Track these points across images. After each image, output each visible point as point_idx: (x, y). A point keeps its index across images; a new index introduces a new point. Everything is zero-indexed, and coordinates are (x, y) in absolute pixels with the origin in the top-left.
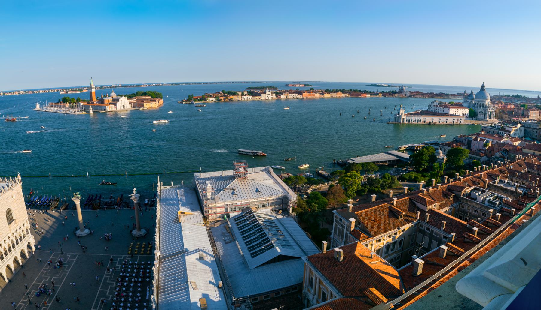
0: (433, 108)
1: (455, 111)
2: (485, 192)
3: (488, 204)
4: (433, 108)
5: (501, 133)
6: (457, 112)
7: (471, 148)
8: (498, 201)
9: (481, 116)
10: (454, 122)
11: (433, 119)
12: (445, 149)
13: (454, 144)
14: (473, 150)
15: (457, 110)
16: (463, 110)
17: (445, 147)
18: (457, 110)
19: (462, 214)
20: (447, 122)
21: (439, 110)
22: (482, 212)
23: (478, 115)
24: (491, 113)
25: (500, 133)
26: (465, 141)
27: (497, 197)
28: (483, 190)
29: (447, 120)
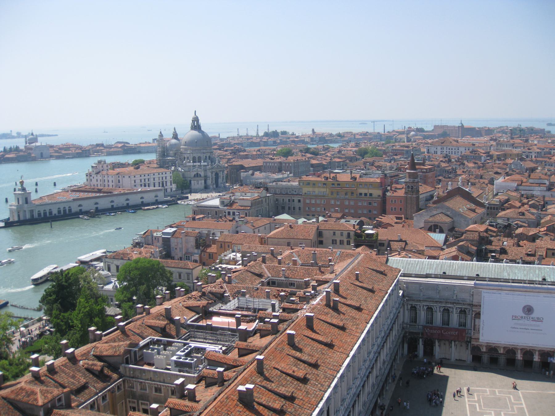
0: (95, 178)
1: (143, 181)
2: (170, 344)
3: (177, 369)
4: (95, 178)
5: (231, 213)
6: (147, 180)
7: (173, 254)
8: (196, 357)
9: (198, 183)
11: (97, 203)
12: (117, 267)
13: (133, 251)
14: (176, 257)
15: (149, 177)
16: (161, 176)
18: (149, 177)
19: (134, 402)
21: (110, 181)
22: (170, 389)
23: (192, 182)
24: (217, 174)
25: (229, 213)
26: (158, 241)
27: (198, 350)
28: (167, 341)
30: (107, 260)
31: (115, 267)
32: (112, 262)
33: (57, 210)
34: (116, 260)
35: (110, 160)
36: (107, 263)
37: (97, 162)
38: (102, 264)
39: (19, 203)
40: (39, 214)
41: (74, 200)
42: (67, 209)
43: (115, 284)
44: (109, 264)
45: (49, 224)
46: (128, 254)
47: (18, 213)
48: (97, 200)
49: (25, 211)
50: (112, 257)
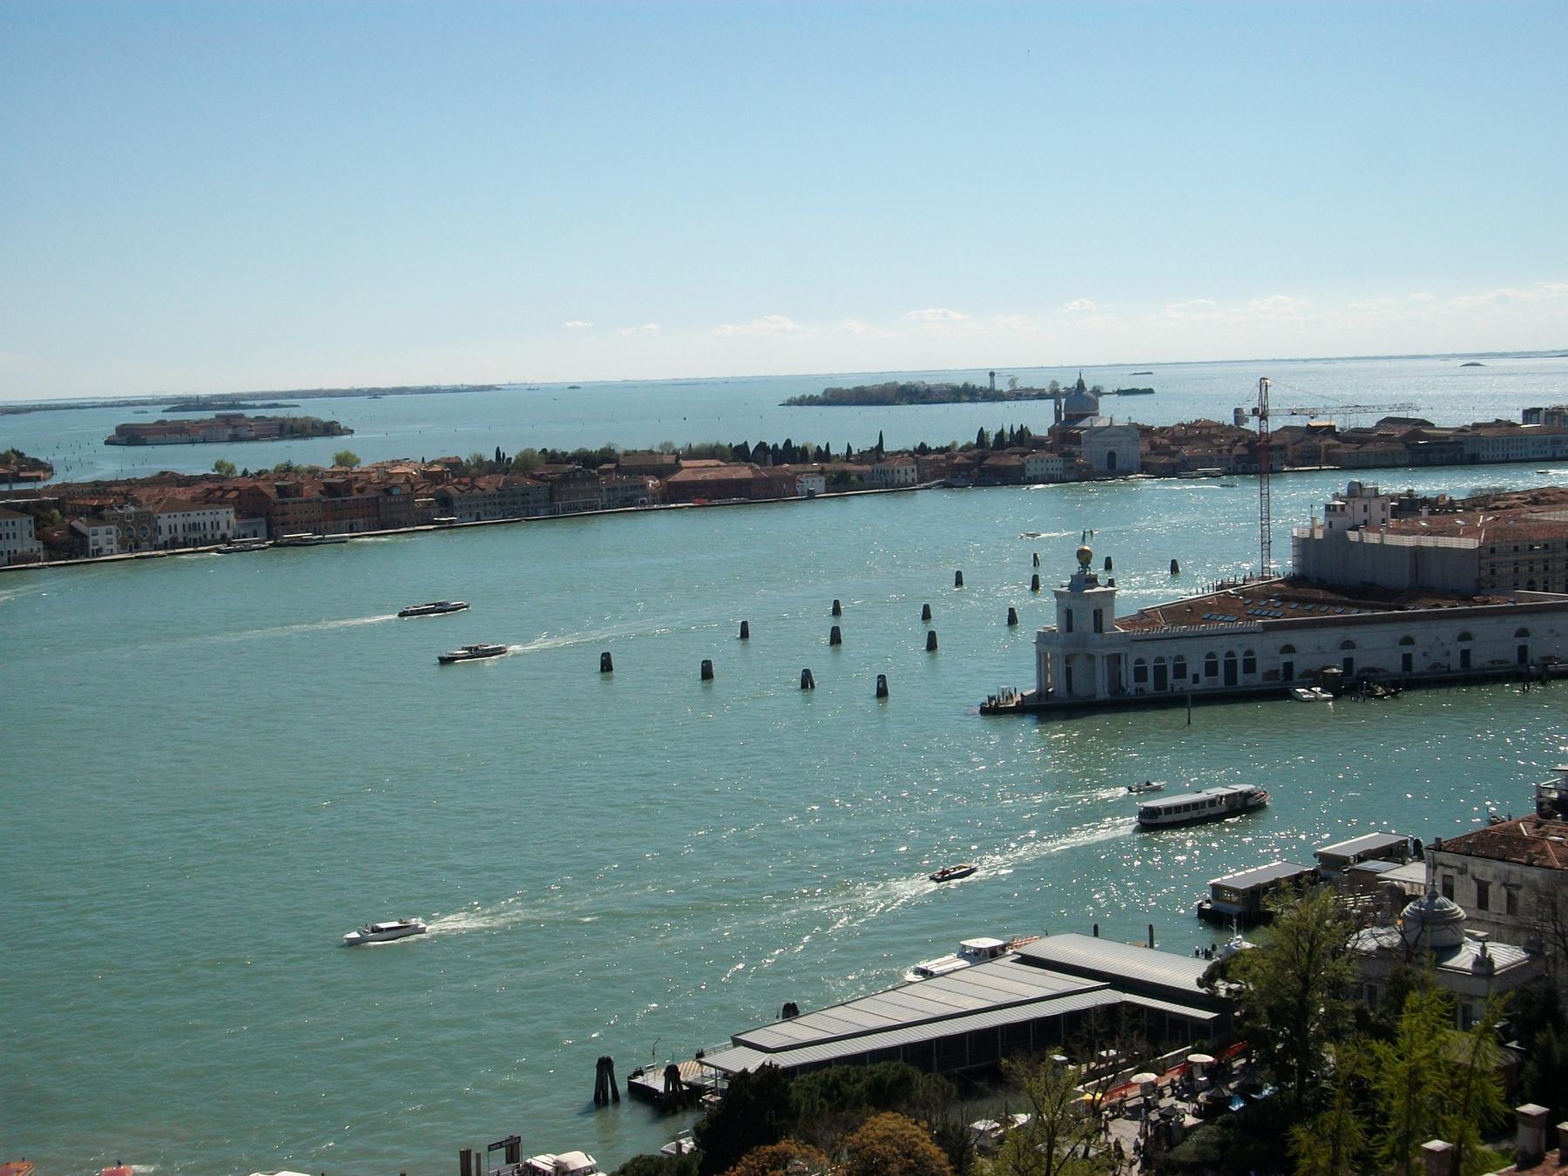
1: (1523, 569)
10: (1523, 651)
11: (1348, 645)
13: (1544, 834)
17: (1479, 867)
20: (1465, 654)
29: (1465, 645)
30: (1441, 856)
31: (1474, 886)
32: (1459, 864)
33: (1204, 660)
34: (1478, 861)
35: (1392, 484)
36: (1440, 868)
37: (1342, 490)
38: (1413, 874)
39: (1069, 628)
40: (1140, 674)
41: (1267, 628)
42: (1240, 659)
43: (1484, 949)
44: (1449, 872)
45: (1186, 710)
46: (1526, 842)
47: (1067, 661)
48: (1352, 633)
49: (1091, 657)
50: (1463, 848)
